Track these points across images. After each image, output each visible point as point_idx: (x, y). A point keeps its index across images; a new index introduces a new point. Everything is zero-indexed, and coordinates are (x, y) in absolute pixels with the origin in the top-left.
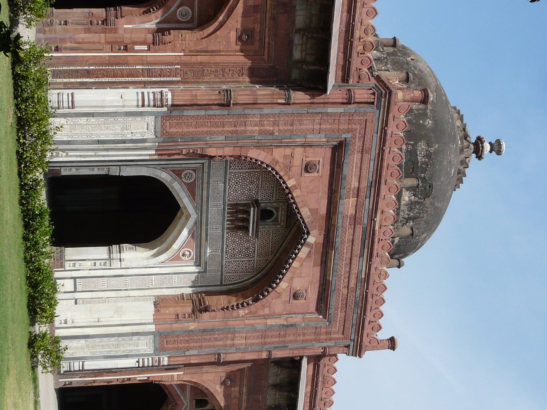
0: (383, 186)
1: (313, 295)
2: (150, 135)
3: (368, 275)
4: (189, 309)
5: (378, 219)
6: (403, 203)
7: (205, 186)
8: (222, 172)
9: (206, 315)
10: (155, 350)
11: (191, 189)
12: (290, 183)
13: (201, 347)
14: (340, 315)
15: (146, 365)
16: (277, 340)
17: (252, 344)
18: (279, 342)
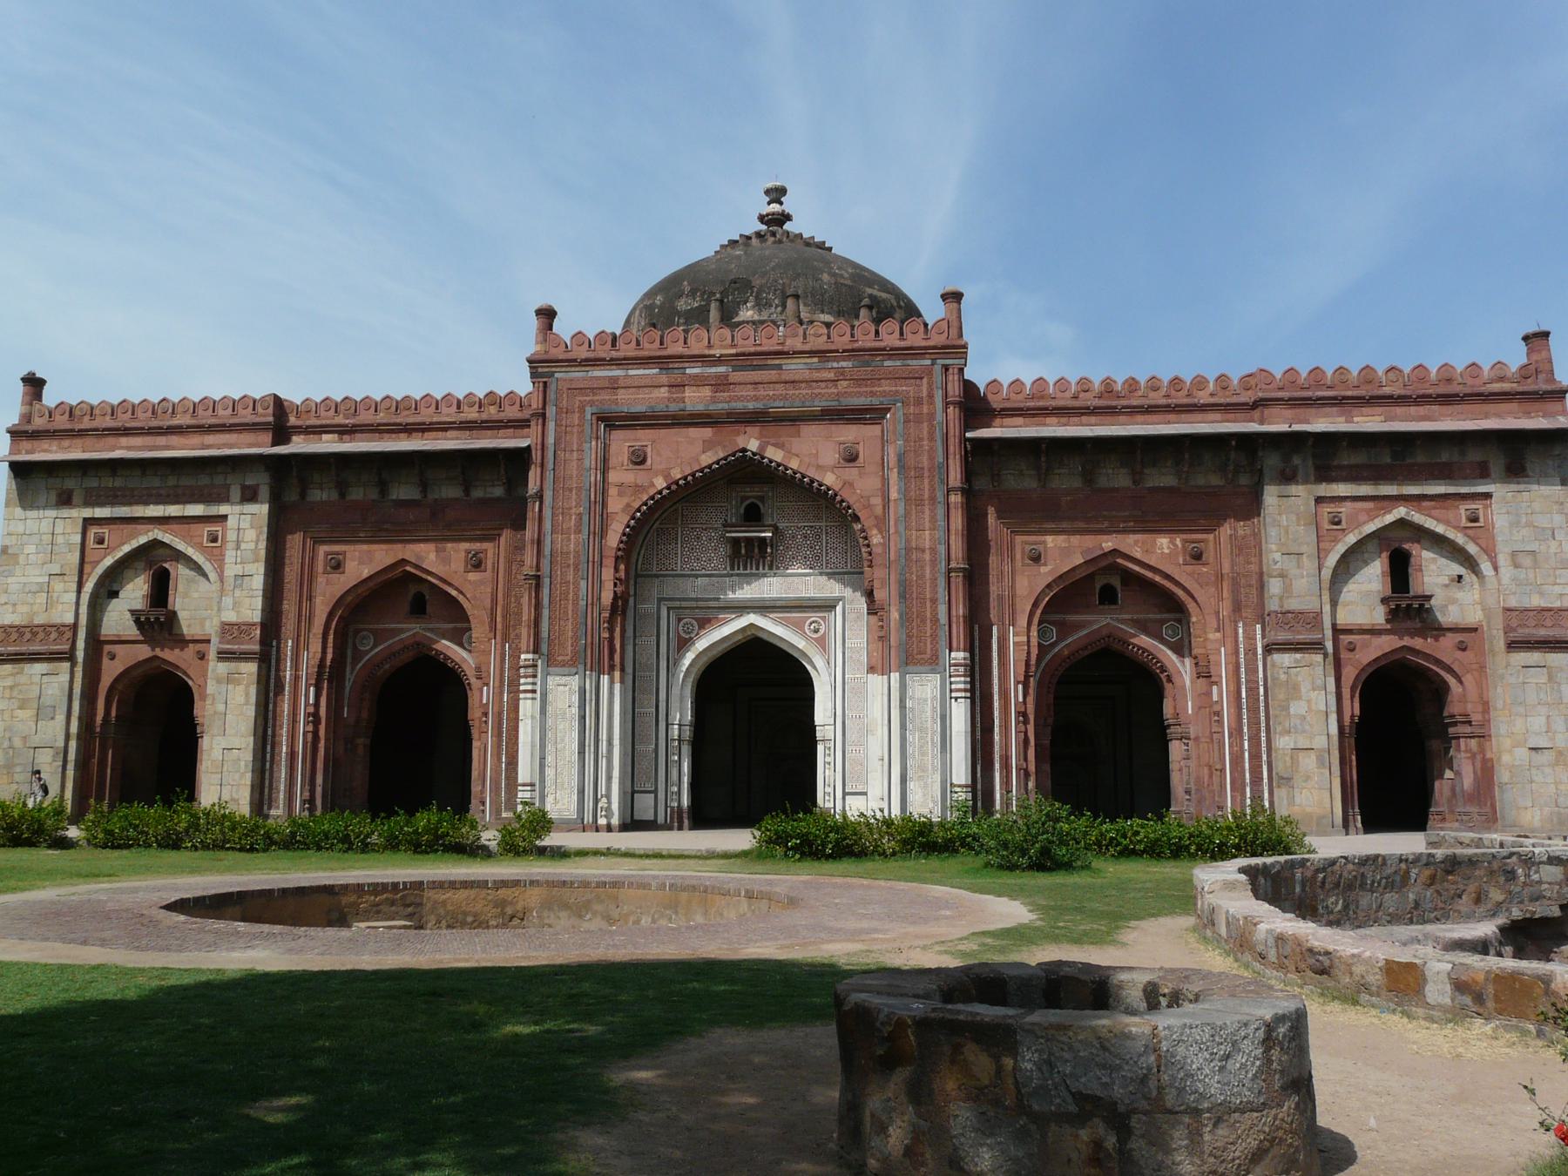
0: (669, 352)
1: (849, 433)
2: (575, 682)
3: (812, 353)
4: (874, 619)
5: (717, 352)
6: (756, 317)
7: (701, 604)
8: (680, 581)
9: (879, 595)
10: (933, 672)
11: (704, 623)
12: (660, 483)
13: (934, 601)
14: (886, 387)
15: (962, 686)
16: (926, 481)
17: (933, 519)
18: (931, 478)
